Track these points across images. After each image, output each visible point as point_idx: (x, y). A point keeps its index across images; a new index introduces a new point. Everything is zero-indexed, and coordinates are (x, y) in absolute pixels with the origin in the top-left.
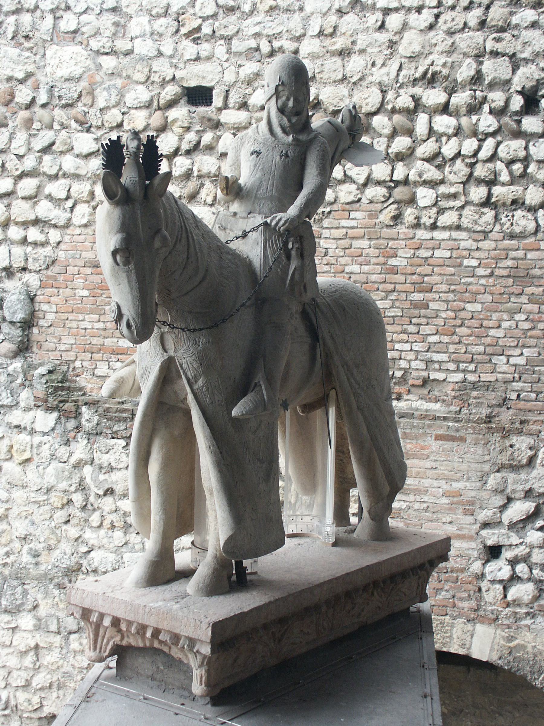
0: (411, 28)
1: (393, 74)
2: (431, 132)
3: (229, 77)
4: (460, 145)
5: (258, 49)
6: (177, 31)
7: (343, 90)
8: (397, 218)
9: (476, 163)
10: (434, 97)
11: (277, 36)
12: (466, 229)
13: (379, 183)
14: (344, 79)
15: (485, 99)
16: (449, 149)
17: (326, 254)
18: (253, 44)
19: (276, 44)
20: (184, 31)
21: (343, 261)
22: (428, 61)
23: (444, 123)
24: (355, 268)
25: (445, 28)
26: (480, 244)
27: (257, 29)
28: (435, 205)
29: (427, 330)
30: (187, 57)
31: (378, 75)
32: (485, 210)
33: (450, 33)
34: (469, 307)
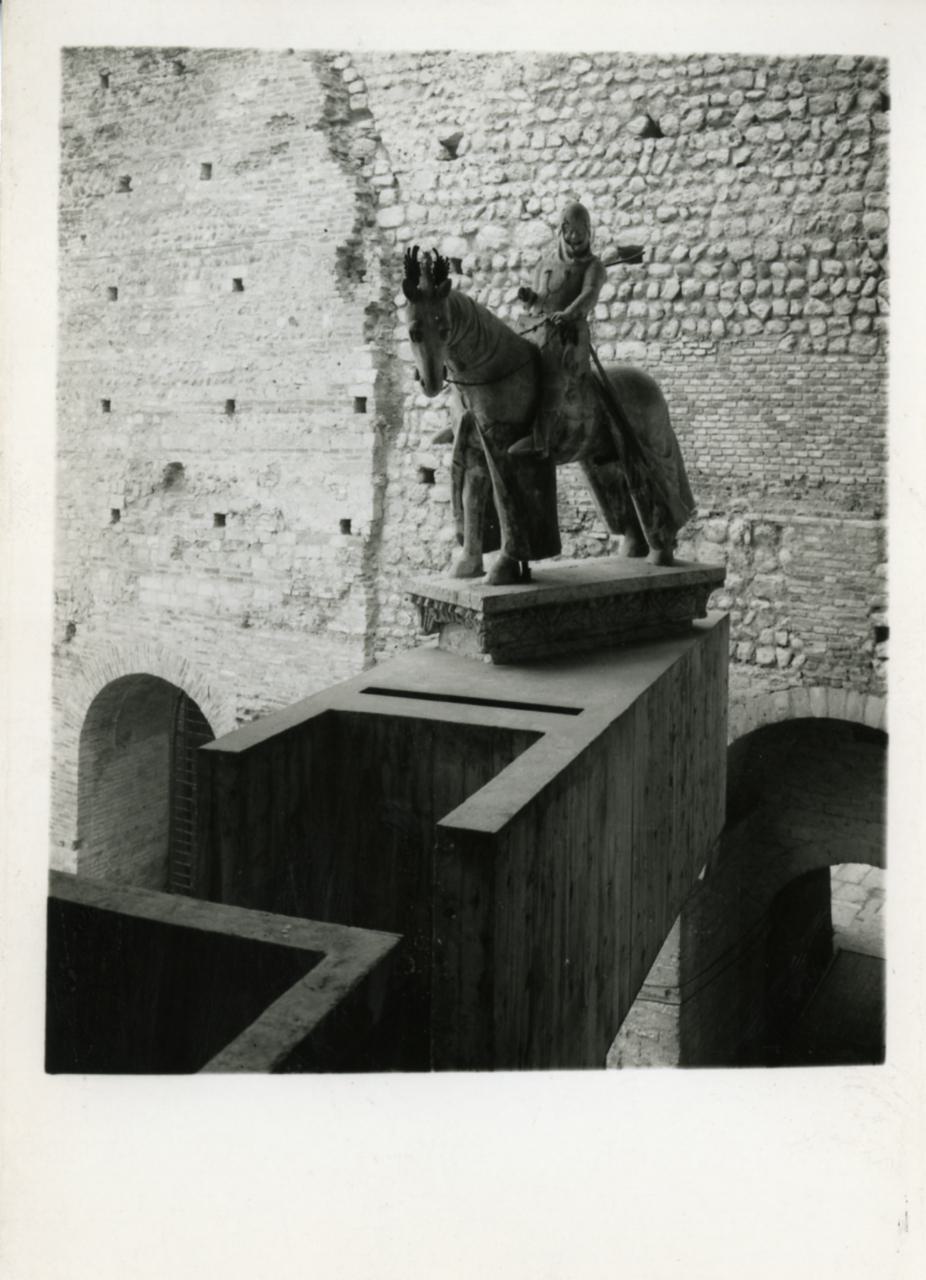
0: (802, 191)
1: (787, 229)
2: (821, 273)
3: (656, 237)
4: (846, 284)
5: (678, 214)
6: (615, 205)
7: (747, 243)
8: (794, 345)
9: (859, 298)
10: (823, 244)
11: (693, 204)
12: (853, 354)
13: (780, 317)
14: (747, 234)
15: (865, 246)
16: (836, 287)
17: (734, 378)
18: (673, 210)
19: (693, 210)
20: (620, 204)
21: (749, 382)
22: (816, 217)
23: (830, 266)
24: (759, 388)
25: (830, 189)
26: (866, 366)
27: (677, 199)
28: (825, 333)
29: (822, 439)
30: (623, 224)
31: (775, 229)
32: (869, 337)
33: (834, 193)
34: (858, 419)
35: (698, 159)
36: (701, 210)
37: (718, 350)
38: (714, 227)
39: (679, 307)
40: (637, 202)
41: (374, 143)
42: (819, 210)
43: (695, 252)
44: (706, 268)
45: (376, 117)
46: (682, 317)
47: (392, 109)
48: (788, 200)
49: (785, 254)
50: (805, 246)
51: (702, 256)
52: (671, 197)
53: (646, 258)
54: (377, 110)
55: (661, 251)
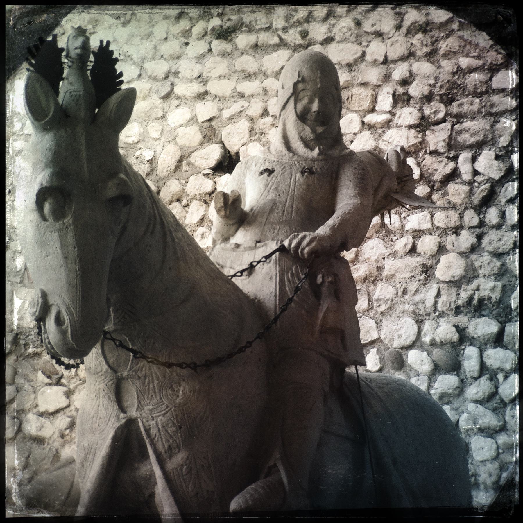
1: (429, 303)
2: (483, 368)
28: (496, 458)
42: (476, 277)
48: (429, 263)
49: (427, 339)
50: (457, 327)
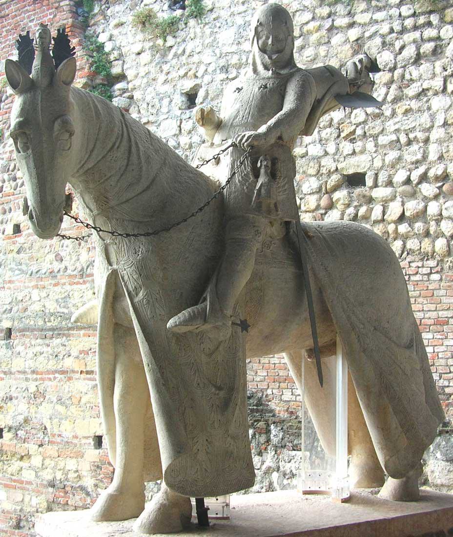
3: (378, 163)
5: (398, 141)
6: (339, 136)
11: (413, 129)
18: (394, 137)
19: (411, 136)
27: (397, 127)
30: (345, 153)
35: (411, 91)
36: (421, 136)
37: (442, 269)
38: (433, 151)
39: (403, 228)
40: (359, 131)
41: (128, 100)
43: (415, 176)
44: (428, 189)
45: (129, 78)
46: (405, 238)
47: (142, 71)
51: (424, 178)
52: (391, 126)
53: (369, 182)
54: (130, 74)
55: (383, 177)
